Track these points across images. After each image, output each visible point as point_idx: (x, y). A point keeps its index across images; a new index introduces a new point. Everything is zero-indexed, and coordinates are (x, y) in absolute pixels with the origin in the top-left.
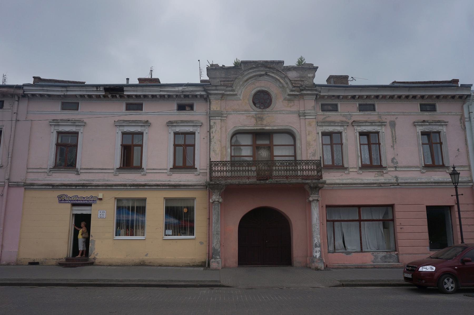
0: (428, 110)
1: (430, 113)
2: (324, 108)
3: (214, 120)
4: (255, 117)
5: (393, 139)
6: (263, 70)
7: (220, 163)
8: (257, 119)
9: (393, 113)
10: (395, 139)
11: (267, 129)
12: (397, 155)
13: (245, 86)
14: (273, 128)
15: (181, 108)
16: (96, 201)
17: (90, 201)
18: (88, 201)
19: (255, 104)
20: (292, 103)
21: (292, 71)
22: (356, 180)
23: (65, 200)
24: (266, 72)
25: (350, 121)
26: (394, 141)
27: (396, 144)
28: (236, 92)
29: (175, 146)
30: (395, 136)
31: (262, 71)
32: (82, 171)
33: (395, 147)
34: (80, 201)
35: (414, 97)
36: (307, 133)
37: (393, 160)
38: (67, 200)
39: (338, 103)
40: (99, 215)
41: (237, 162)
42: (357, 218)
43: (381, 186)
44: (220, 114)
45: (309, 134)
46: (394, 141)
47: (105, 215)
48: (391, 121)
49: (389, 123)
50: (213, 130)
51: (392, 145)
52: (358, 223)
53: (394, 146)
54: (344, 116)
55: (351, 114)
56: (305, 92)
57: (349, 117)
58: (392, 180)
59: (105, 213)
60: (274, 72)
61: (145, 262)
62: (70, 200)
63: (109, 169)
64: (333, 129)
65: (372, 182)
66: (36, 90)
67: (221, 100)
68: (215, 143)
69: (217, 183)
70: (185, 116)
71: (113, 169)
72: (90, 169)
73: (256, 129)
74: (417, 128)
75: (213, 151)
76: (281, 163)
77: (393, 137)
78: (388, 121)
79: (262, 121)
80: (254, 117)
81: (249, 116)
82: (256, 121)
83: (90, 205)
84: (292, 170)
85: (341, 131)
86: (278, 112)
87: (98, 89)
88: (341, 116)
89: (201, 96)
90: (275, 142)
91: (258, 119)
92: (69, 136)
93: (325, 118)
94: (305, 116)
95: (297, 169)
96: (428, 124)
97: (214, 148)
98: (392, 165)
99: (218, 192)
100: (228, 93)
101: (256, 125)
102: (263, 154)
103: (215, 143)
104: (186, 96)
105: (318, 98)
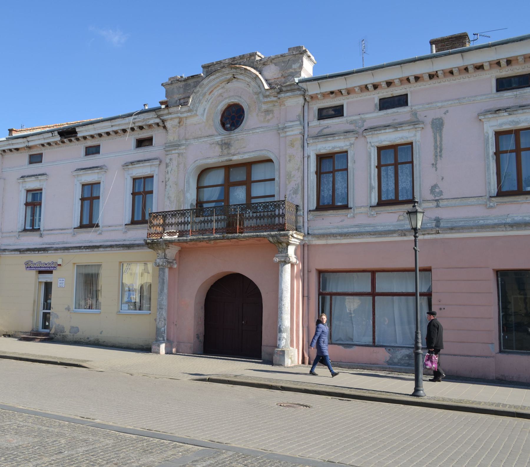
0: (514, 86)
1: (515, 93)
2: (323, 114)
3: (170, 155)
4: (221, 144)
5: (436, 152)
6: (228, 72)
7: (160, 214)
8: (223, 146)
9: (439, 104)
10: (441, 151)
11: (235, 160)
12: (443, 179)
13: (209, 101)
14: (243, 157)
15: (141, 143)
16: (56, 267)
17: (52, 267)
18: (49, 267)
19: (223, 125)
20: (271, 116)
21: (269, 64)
22: (365, 227)
23: (30, 267)
24: (233, 75)
25: (361, 131)
26: (439, 154)
27: (441, 159)
28: (195, 112)
29: (134, 194)
30: (441, 143)
31: (227, 74)
32: (45, 232)
33: (439, 166)
34: (43, 267)
35: (479, 67)
36: (288, 159)
37: (433, 188)
38: (32, 267)
39: (343, 103)
40: (59, 284)
41: (179, 212)
42: (369, 290)
43: (405, 235)
44: (176, 146)
45: (290, 160)
46: (439, 154)
47: (64, 284)
48: (436, 119)
49: (431, 123)
50: (169, 169)
51: (433, 162)
52: (370, 298)
53: (436, 164)
54: (351, 123)
55: (362, 116)
56: (282, 95)
57: (360, 124)
58: (428, 225)
59: (64, 281)
60: (241, 72)
61: (99, 341)
62: (34, 267)
63: (68, 229)
64: (333, 146)
65: (392, 228)
66: (4, 146)
67: (179, 127)
68: (170, 187)
69: (155, 242)
70: (145, 152)
71: (121, 225)
72: (52, 230)
73: (221, 161)
74: (485, 125)
75: (168, 198)
76: (264, 207)
77: (436, 149)
78: (428, 120)
79: (229, 148)
80: (218, 144)
81: (213, 144)
82: (222, 149)
83: (51, 272)
84: (268, 217)
85: (345, 149)
86: (251, 132)
87: (53, 135)
88: (347, 123)
89: (158, 124)
90: (254, 177)
91: (224, 146)
92: (38, 193)
93: (321, 130)
94: (286, 132)
95: (275, 214)
96: (506, 114)
97: (168, 194)
98: (431, 197)
99: (162, 254)
100: (185, 115)
101: (221, 156)
102: (240, 196)
103: (170, 187)
104: (141, 128)
105: (308, 99)
